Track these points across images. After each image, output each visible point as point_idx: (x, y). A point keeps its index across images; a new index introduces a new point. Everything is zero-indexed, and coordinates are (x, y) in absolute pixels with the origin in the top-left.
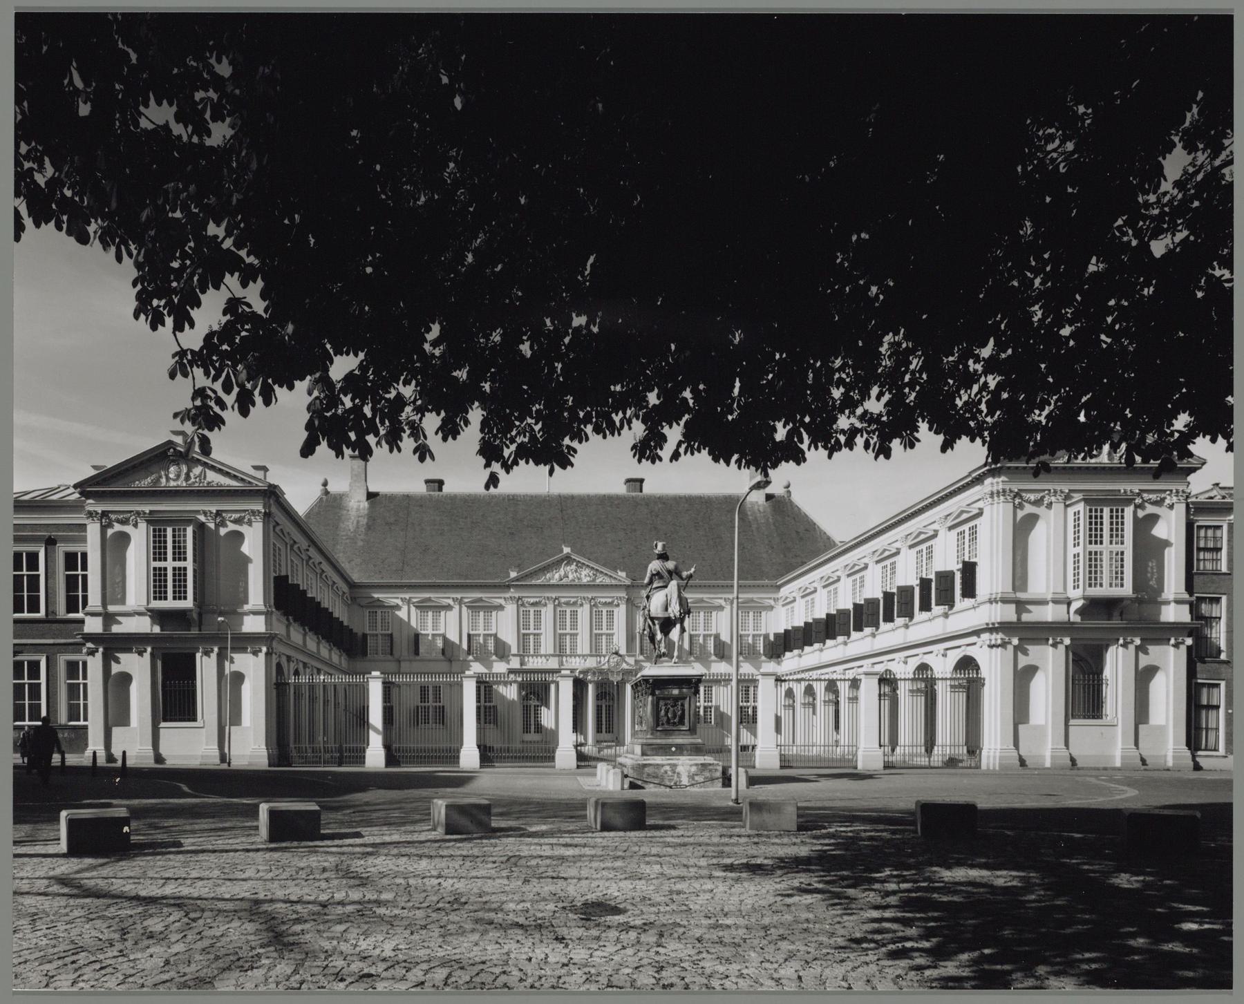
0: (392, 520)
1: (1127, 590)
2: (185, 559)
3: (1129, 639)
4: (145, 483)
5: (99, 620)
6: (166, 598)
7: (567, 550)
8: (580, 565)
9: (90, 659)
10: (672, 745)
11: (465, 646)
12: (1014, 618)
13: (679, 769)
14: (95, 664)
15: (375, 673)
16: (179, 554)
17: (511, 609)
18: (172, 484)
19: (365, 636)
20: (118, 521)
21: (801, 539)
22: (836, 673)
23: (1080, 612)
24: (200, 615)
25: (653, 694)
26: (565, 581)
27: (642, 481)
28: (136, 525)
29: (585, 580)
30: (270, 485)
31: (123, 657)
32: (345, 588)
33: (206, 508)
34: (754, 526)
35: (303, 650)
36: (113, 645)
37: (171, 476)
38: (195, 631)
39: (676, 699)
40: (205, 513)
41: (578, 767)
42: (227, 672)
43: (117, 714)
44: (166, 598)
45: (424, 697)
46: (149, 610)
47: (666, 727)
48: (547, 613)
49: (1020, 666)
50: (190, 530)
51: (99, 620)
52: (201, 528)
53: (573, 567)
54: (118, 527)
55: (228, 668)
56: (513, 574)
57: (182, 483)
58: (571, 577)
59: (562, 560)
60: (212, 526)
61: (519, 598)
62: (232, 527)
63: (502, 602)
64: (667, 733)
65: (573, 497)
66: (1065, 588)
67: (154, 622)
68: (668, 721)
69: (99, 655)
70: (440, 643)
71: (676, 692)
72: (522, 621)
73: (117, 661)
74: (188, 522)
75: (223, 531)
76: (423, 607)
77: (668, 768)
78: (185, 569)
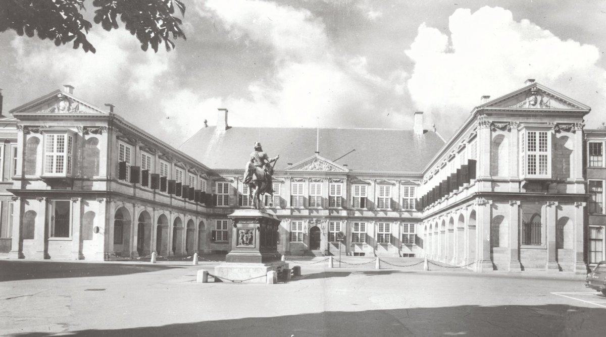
2: (63, 151)
3: (514, 202)
5: (20, 182)
12: (490, 190)
18: (61, 112)
23: (524, 187)
26: (313, 170)
36: (24, 195)
37: (61, 108)
49: (494, 216)
50: (66, 136)
51: (20, 182)
57: (65, 113)
58: (317, 168)
60: (81, 134)
62: (91, 135)
66: (518, 175)
67: (48, 185)
73: (28, 204)
74: (65, 132)
75: (87, 137)
78: (63, 157)
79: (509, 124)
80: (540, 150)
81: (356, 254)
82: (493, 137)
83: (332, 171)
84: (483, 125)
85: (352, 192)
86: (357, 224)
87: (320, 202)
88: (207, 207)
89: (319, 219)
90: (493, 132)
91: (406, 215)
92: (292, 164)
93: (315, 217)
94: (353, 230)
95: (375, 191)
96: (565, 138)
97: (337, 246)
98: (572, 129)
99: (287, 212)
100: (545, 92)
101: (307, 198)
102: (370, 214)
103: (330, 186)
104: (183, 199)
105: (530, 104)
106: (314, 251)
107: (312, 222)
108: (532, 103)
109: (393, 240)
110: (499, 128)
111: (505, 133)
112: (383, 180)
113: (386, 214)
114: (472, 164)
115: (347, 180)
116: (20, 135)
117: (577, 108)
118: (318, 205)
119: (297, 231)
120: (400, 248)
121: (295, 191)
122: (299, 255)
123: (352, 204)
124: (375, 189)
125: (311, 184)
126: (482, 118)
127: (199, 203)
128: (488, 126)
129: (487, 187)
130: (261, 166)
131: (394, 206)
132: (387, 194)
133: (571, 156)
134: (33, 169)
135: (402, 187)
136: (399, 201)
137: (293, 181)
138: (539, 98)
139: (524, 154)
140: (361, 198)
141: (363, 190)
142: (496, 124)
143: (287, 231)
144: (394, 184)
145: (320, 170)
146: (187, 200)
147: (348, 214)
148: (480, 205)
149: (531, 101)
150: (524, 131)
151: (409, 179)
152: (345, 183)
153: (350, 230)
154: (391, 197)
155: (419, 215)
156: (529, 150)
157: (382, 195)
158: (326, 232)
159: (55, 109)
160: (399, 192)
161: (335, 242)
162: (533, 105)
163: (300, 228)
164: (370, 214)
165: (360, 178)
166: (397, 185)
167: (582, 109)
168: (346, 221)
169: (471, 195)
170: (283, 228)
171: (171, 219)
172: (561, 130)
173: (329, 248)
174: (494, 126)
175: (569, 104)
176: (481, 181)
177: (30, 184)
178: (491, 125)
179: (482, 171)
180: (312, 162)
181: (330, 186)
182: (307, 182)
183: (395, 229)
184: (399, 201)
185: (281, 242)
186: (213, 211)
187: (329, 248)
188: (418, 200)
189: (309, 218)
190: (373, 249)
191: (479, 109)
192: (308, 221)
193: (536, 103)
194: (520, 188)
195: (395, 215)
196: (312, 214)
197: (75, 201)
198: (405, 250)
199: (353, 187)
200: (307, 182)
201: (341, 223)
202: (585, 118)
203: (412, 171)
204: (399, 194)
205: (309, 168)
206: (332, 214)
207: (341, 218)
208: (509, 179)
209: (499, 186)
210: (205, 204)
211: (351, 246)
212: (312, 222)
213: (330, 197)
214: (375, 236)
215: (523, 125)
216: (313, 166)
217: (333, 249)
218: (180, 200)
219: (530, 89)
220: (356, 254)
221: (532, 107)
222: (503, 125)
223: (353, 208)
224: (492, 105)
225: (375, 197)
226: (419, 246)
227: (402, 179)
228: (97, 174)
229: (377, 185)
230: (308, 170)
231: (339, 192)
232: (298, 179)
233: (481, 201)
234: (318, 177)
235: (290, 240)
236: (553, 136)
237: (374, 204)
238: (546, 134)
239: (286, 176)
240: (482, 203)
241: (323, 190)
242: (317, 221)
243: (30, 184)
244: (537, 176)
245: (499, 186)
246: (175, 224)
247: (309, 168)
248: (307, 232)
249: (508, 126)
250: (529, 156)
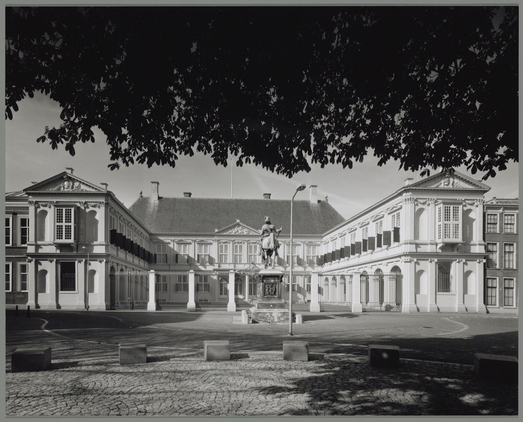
0: (168, 208)
2: (71, 222)
4: (53, 190)
6: (62, 238)
7: (238, 221)
8: (244, 227)
9: (29, 264)
10: (271, 304)
11: (196, 259)
13: (274, 314)
14: (31, 267)
15: (152, 271)
16: (68, 220)
17: (215, 244)
18: (66, 190)
19: (155, 255)
20: (42, 205)
21: (332, 218)
22: (345, 272)
24: (77, 246)
25: (263, 282)
26: (237, 234)
27: (270, 195)
28: (50, 207)
29: (245, 233)
30: (108, 191)
31: (43, 262)
32: (147, 235)
33: (80, 201)
34: (313, 213)
35: (125, 261)
36: (39, 258)
37: (66, 187)
38: (75, 253)
39: (273, 284)
40: (80, 203)
41: (237, 311)
42: (39, 270)
43: (40, 287)
44: (62, 238)
45: (180, 280)
46: (55, 244)
47: (268, 296)
48: (230, 246)
50: (73, 210)
52: (78, 209)
53: (240, 228)
54: (42, 208)
55: (90, 268)
56: (216, 231)
57: (70, 190)
58: (239, 232)
59: (236, 225)
61: (219, 240)
62: (91, 209)
63: (212, 241)
64: (268, 299)
65: (241, 200)
68: (269, 294)
69: (33, 263)
70: (186, 257)
71: (272, 281)
72: (220, 249)
73: (41, 264)
74: (72, 206)
75: (87, 210)
76: (180, 243)
77: (268, 314)
78: (70, 226)
82: (416, 210)
96: (470, 211)
108: (446, 183)
116: (32, 209)
133: (474, 223)
134: (42, 238)
142: (418, 200)
150: (441, 206)
159: (61, 187)
162: (447, 185)
177: (42, 248)
179: (406, 234)
197: (80, 262)
202: (484, 195)
221: (446, 187)
222: (425, 201)
228: (97, 240)
243: (42, 248)
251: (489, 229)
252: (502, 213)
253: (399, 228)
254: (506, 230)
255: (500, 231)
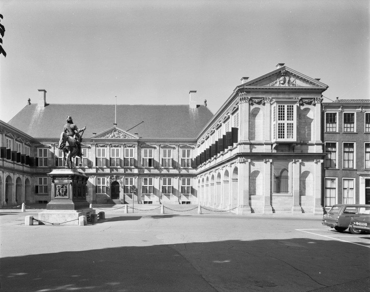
1: (294, 139)
12: (249, 151)
23: (275, 148)
26: (113, 138)
58: (116, 136)
79: (264, 99)
80: (288, 119)
81: (145, 202)
82: (251, 110)
83: (126, 138)
84: (243, 101)
85: (142, 155)
86: (146, 180)
87: (119, 163)
88: (31, 168)
89: (118, 176)
90: (251, 106)
91: (184, 172)
92: (96, 134)
93: (115, 174)
94: (143, 184)
95: (159, 153)
96: (307, 110)
97: (131, 196)
98: (313, 103)
99: (93, 171)
100: (292, 74)
101: (109, 159)
102: (156, 171)
103: (125, 150)
104: (12, 162)
105: (280, 83)
106: (114, 200)
107: (112, 178)
108: (282, 82)
109: (174, 191)
110: (256, 103)
111: (261, 106)
112: (166, 145)
113: (169, 171)
114: (235, 131)
115: (138, 145)
117: (317, 86)
118: (117, 165)
119: (101, 185)
120: (180, 197)
121: (99, 155)
122: (103, 203)
123: (142, 164)
124: (159, 152)
125: (111, 148)
126: (243, 95)
127: (24, 164)
128: (247, 101)
129: (246, 149)
130: (72, 136)
131: (175, 165)
132: (169, 156)
133: (312, 124)
135: (181, 150)
136: (178, 161)
137: (98, 147)
138: (287, 78)
139: (275, 123)
140: (149, 159)
141: (151, 153)
143: (93, 185)
144: (174, 148)
145: (118, 138)
146: (15, 162)
147: (139, 171)
148: (241, 163)
149: (281, 81)
150: (275, 105)
151: (186, 144)
152: (136, 148)
153: (141, 184)
154: (172, 158)
155: (194, 171)
156: (279, 119)
157: (165, 156)
158: (123, 186)
160: (179, 153)
161: (129, 193)
162: (283, 84)
163: (103, 183)
164: (156, 171)
165: (147, 143)
166: (177, 148)
167: (321, 87)
168: (138, 177)
169: (234, 155)
170: (90, 183)
171: (3, 177)
172: (304, 104)
173: (124, 198)
174: (252, 101)
175: (311, 83)
176: (242, 144)
178: (249, 100)
179: (242, 136)
180: (112, 132)
181: (125, 150)
182: (108, 148)
183: (176, 183)
184: (178, 161)
185: (89, 193)
186: (36, 170)
187: (124, 198)
188: (193, 160)
189: (111, 175)
190: (158, 198)
191: (240, 88)
192: (110, 177)
193: (285, 82)
194: (272, 149)
195: (175, 171)
196: (112, 172)
198: (184, 199)
199: (143, 151)
200: (108, 148)
201: (134, 179)
202: (323, 94)
203: (188, 137)
204: (179, 155)
205: (110, 136)
206: (126, 172)
207: (134, 175)
208: (263, 142)
209: (256, 148)
210: (30, 165)
211: (142, 197)
212: (112, 178)
213: (124, 159)
214: (160, 188)
215: (274, 100)
216: (113, 135)
217: (128, 199)
218: (10, 162)
219: (280, 71)
220: (145, 202)
221: (282, 86)
222: (259, 100)
223: (143, 167)
224: (250, 85)
225: (159, 158)
226: (194, 195)
227: (180, 144)
229: (161, 149)
230: (109, 138)
231: (132, 155)
232: (101, 145)
233: (242, 160)
234: (116, 144)
235: (97, 192)
236: (298, 108)
237: (159, 163)
238: (293, 106)
239: (92, 143)
240: (242, 161)
241: (121, 153)
242: (117, 178)
244: (286, 140)
245: (256, 148)
246: (7, 181)
247: (110, 136)
248: (109, 186)
249: (263, 101)
250: (279, 124)
251: (328, 129)
252: (342, 112)
253: (237, 129)
254: (345, 129)
255: (339, 131)
